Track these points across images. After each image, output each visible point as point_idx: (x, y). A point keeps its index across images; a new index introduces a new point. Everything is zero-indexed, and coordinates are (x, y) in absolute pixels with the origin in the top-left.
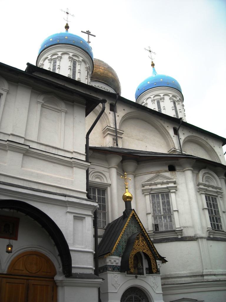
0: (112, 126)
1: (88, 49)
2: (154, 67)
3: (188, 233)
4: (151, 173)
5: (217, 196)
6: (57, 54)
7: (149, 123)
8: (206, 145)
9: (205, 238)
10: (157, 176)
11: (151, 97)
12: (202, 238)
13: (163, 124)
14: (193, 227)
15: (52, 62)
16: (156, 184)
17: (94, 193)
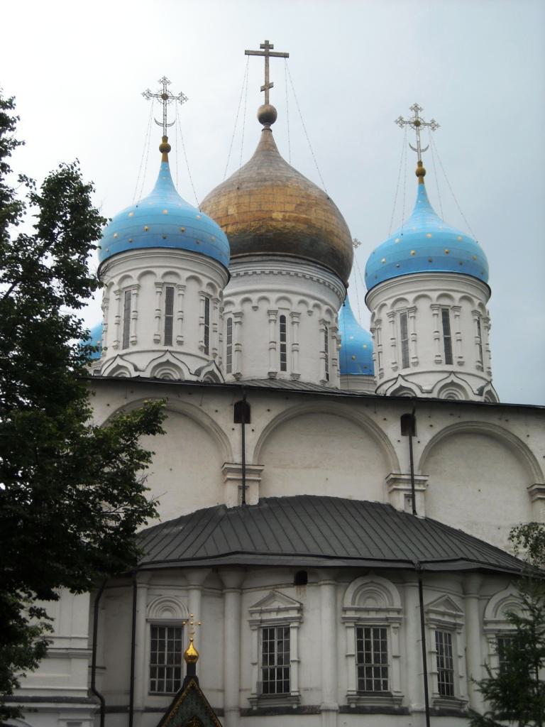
0: (238, 459)
1: (202, 241)
2: (425, 178)
3: (308, 700)
4: (265, 588)
5: (389, 626)
7: (340, 416)
8: (505, 437)
9: (333, 711)
10: (272, 597)
11: (386, 302)
12: (328, 711)
13: (373, 417)
14: (319, 690)
16: (270, 611)
17: (162, 636)
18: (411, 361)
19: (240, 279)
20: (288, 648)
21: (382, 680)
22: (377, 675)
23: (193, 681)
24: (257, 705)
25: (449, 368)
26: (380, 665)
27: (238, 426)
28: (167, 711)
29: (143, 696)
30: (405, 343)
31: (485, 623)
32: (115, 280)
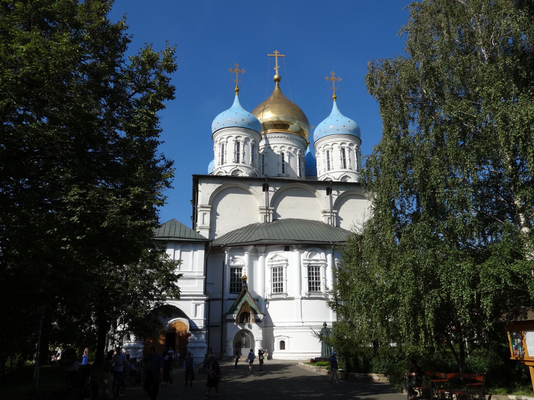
18: (331, 168)
20: (282, 275)
22: (316, 285)
25: (345, 170)
26: (318, 281)
27: (265, 192)
30: (328, 162)
32: (218, 140)
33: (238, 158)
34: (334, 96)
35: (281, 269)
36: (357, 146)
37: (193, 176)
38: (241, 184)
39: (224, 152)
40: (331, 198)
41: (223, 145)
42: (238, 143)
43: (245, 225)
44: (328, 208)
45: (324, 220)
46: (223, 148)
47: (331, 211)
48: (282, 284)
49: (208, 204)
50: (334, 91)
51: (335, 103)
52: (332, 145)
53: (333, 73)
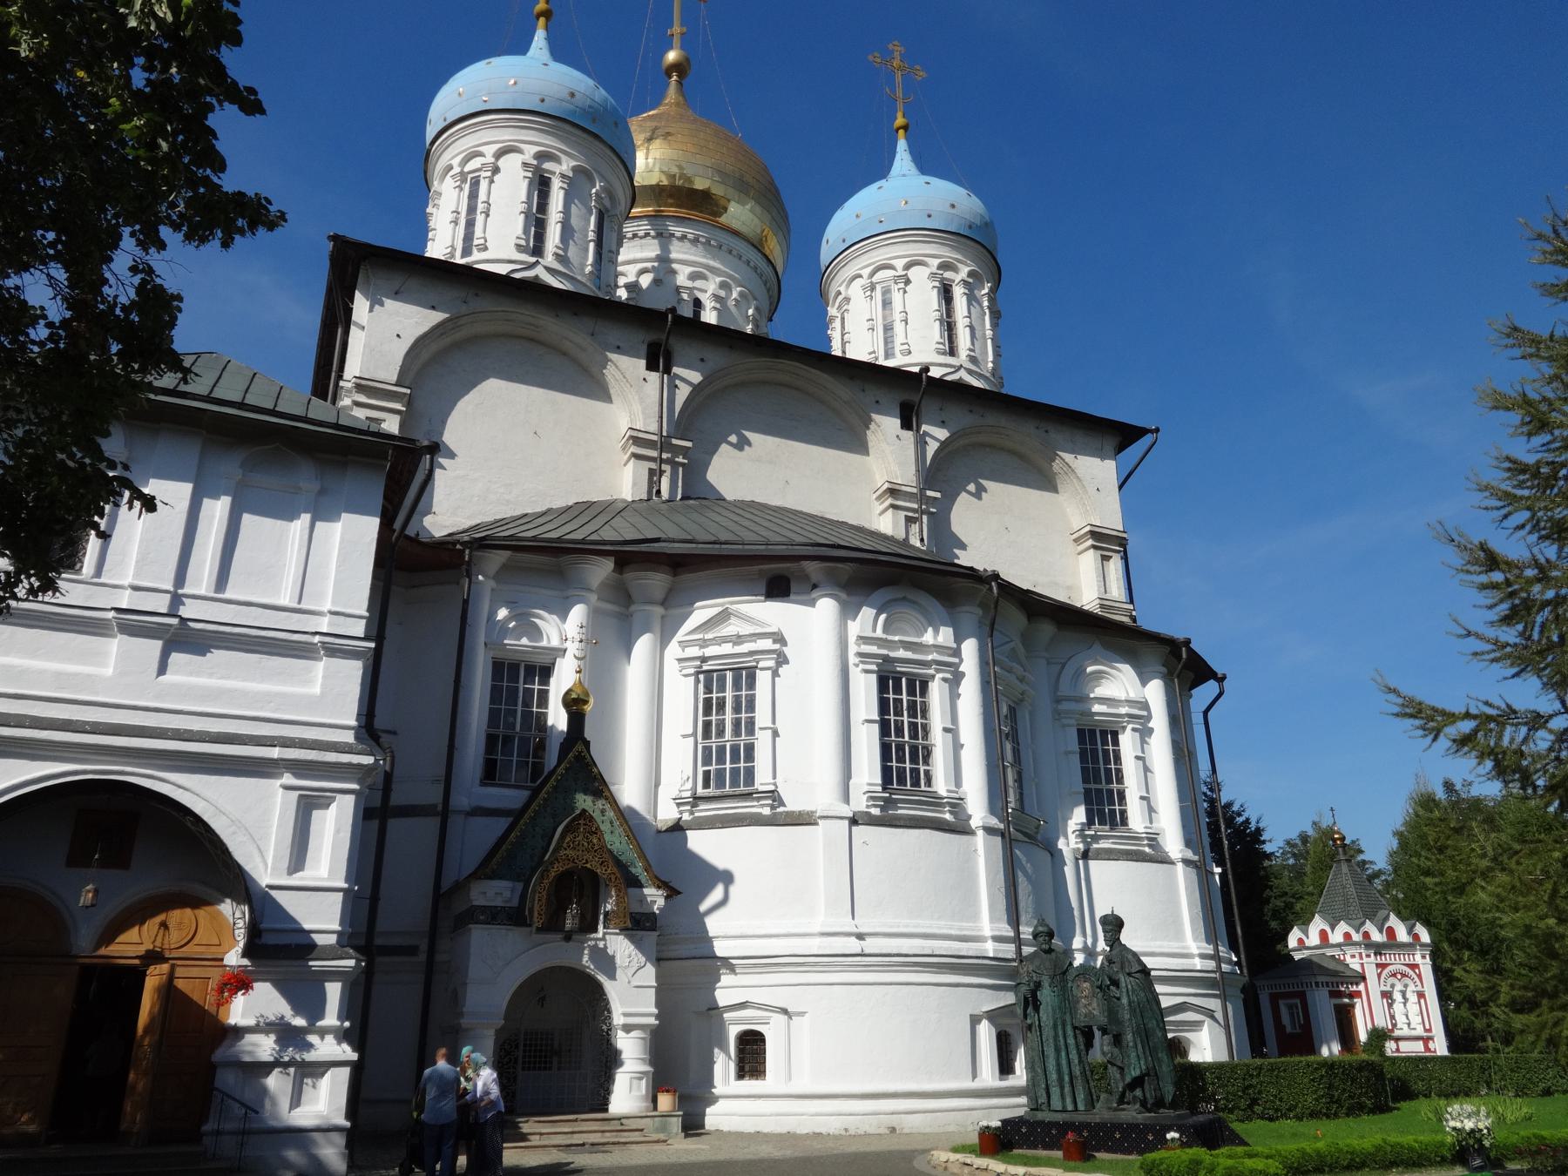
6: (481, 154)
15: (467, 187)
19: (637, 242)
21: (922, 768)
22: (914, 760)
23: (580, 747)
24: (692, 813)
27: (654, 377)
28: (518, 815)
29: (470, 789)
31: (1058, 701)
33: (540, 237)
34: (900, 121)
35: (745, 676)
36: (991, 290)
37: (335, 238)
38: (552, 326)
39: (481, 207)
40: (921, 443)
41: (475, 184)
42: (541, 184)
43: (559, 503)
44: (907, 476)
45: (887, 523)
46: (473, 196)
47: (922, 490)
48: (750, 749)
49: (394, 379)
50: (900, 106)
51: (902, 145)
52: (908, 267)
53: (897, 49)
